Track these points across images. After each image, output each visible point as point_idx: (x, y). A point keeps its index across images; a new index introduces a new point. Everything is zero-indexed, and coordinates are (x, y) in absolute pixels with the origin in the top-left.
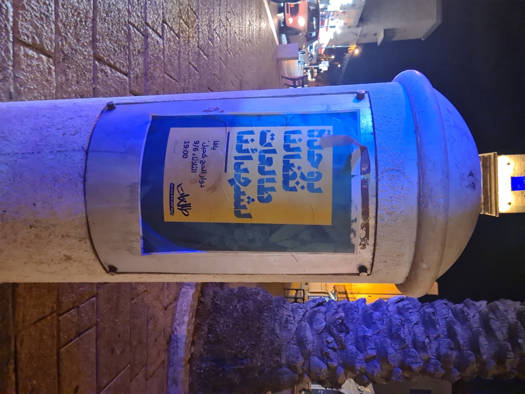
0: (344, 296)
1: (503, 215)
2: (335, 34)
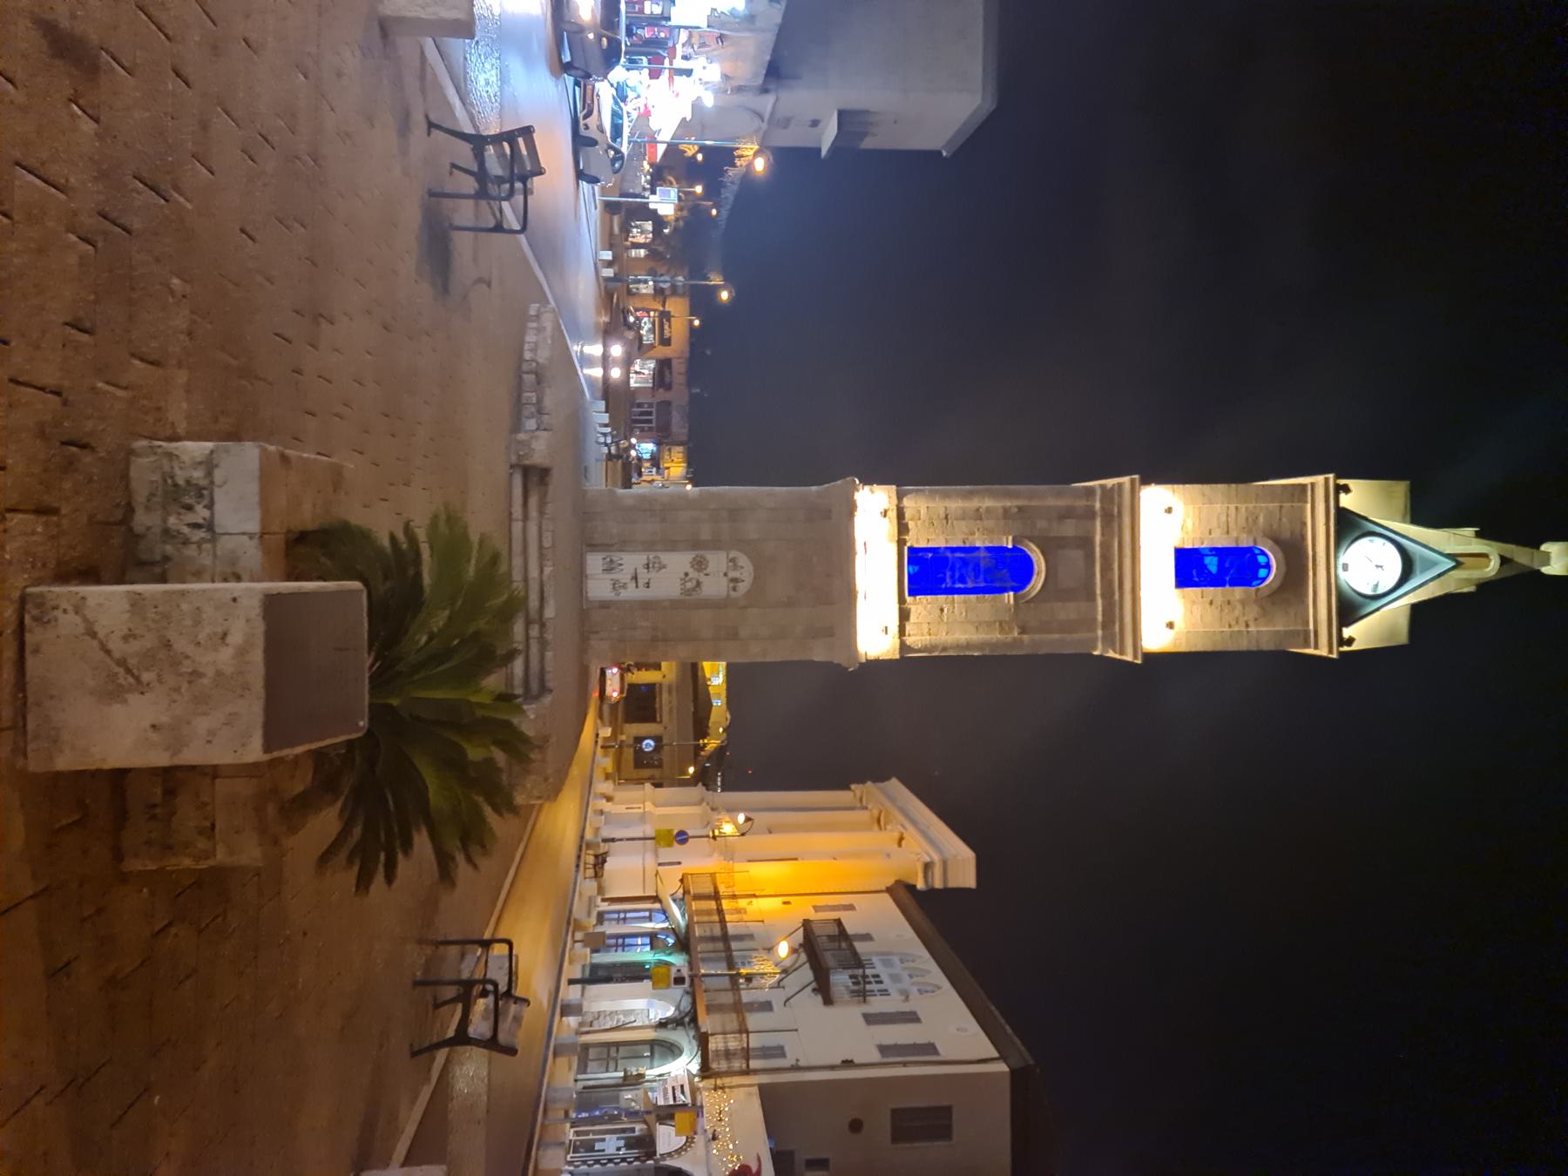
0: (713, 905)
1: (1150, 658)
2: (697, 106)
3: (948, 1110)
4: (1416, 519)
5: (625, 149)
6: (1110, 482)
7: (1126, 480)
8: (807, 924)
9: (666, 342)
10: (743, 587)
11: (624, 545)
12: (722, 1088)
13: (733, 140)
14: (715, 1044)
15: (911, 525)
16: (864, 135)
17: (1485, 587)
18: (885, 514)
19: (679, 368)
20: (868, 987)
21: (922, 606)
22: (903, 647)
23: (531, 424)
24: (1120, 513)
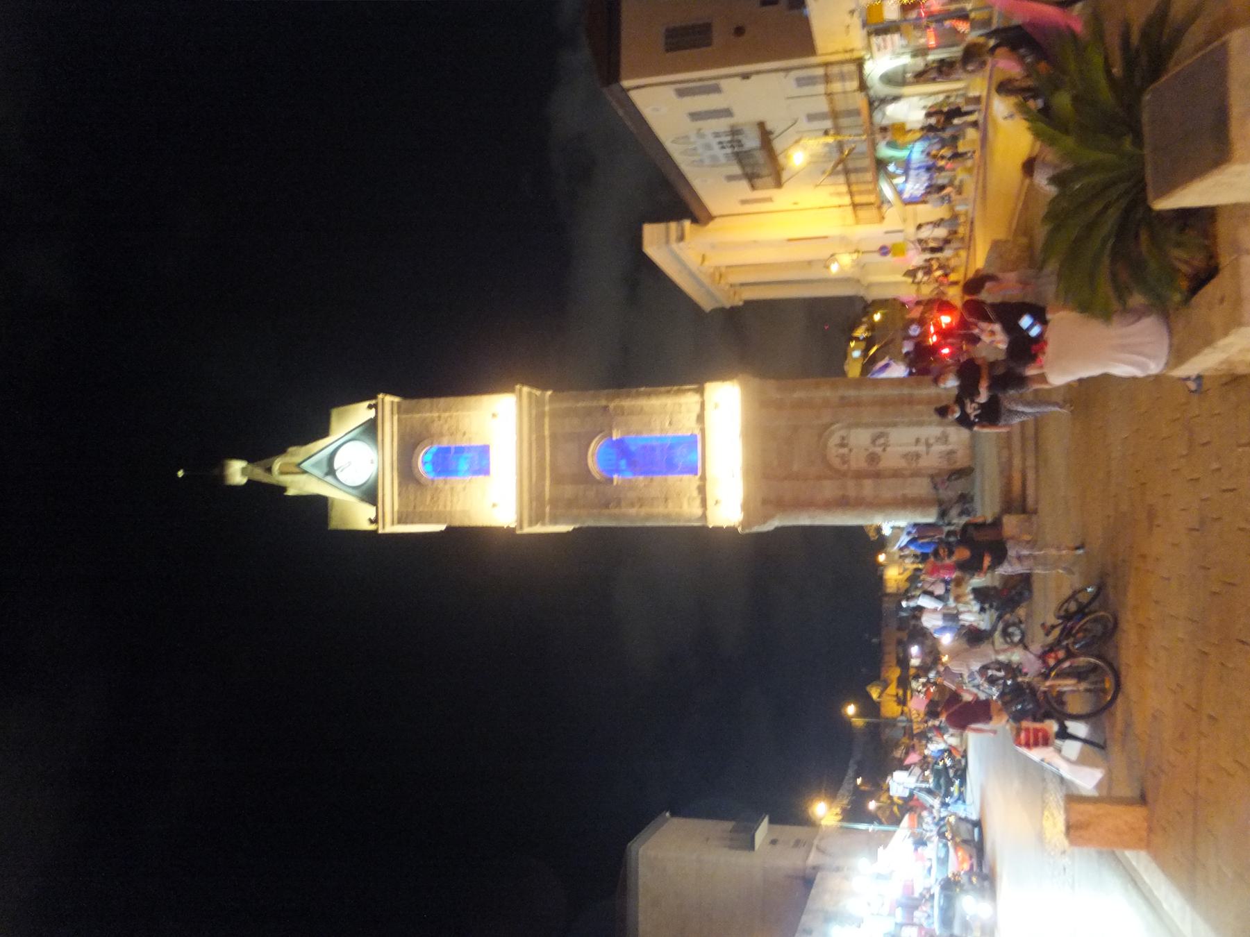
0: (858, 199)
3: (667, 51)
6: (538, 529)
7: (527, 530)
8: (779, 184)
12: (846, 52)
14: (854, 84)
15: (695, 493)
16: (734, 830)
17: (281, 451)
20: (729, 138)
21: (686, 425)
22: (701, 391)
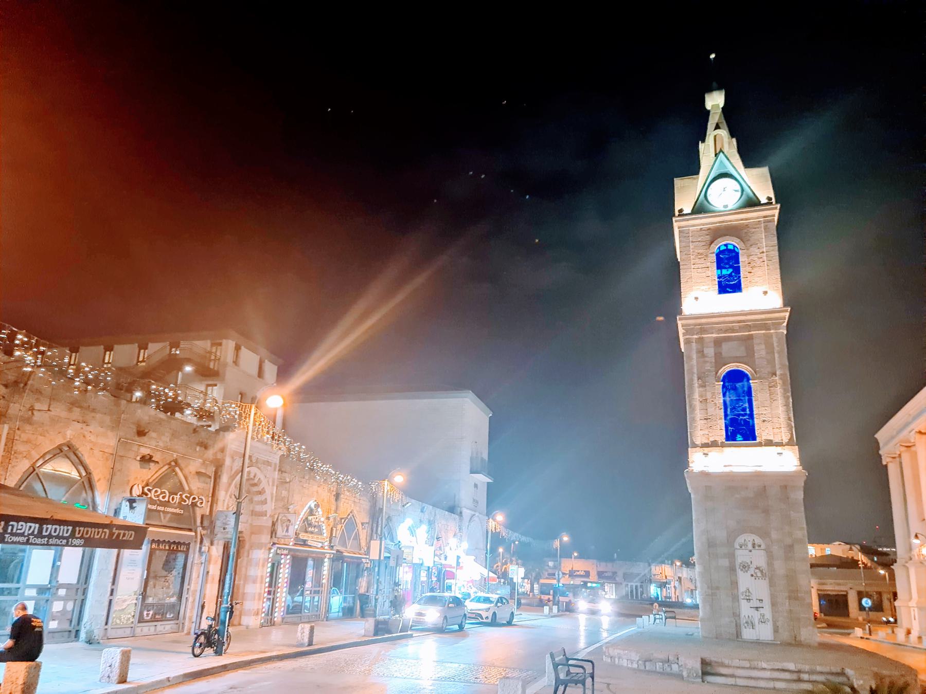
4: (697, 173)
5: (497, 596)
6: (681, 331)
7: (680, 323)
9: (587, 574)
10: (758, 541)
11: (736, 615)
13: (487, 532)
15: (712, 439)
16: (482, 459)
17: (732, 134)
18: (706, 454)
19: (603, 567)
21: (762, 431)
23: (675, 667)
24: (699, 325)
